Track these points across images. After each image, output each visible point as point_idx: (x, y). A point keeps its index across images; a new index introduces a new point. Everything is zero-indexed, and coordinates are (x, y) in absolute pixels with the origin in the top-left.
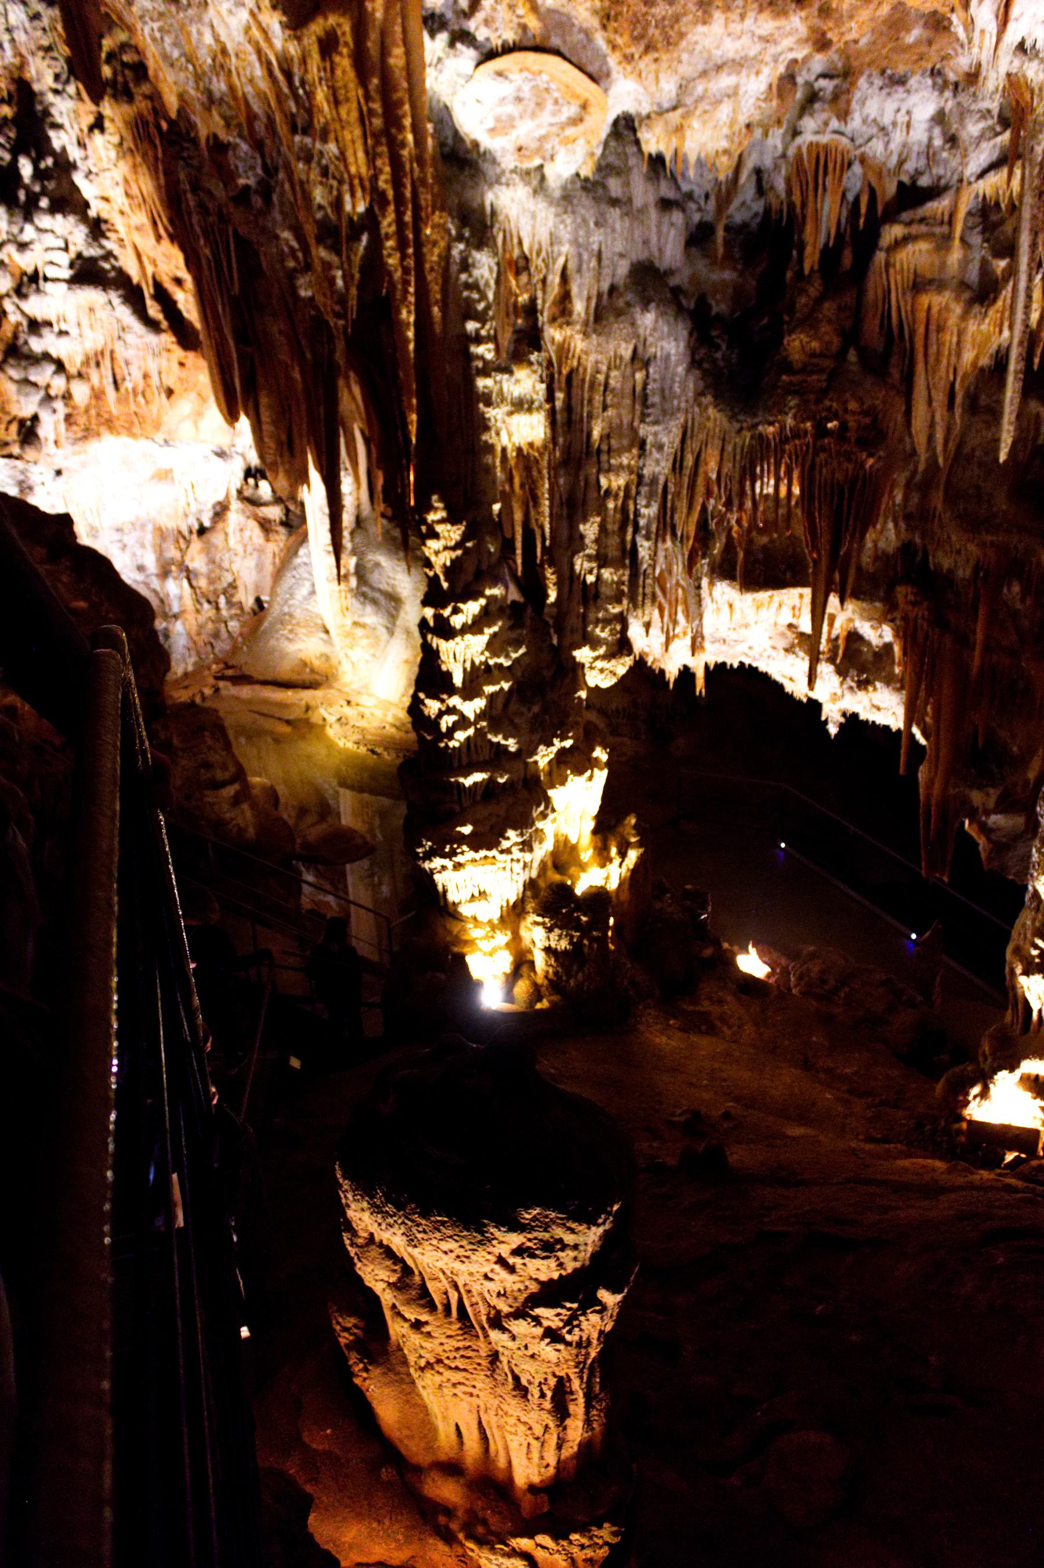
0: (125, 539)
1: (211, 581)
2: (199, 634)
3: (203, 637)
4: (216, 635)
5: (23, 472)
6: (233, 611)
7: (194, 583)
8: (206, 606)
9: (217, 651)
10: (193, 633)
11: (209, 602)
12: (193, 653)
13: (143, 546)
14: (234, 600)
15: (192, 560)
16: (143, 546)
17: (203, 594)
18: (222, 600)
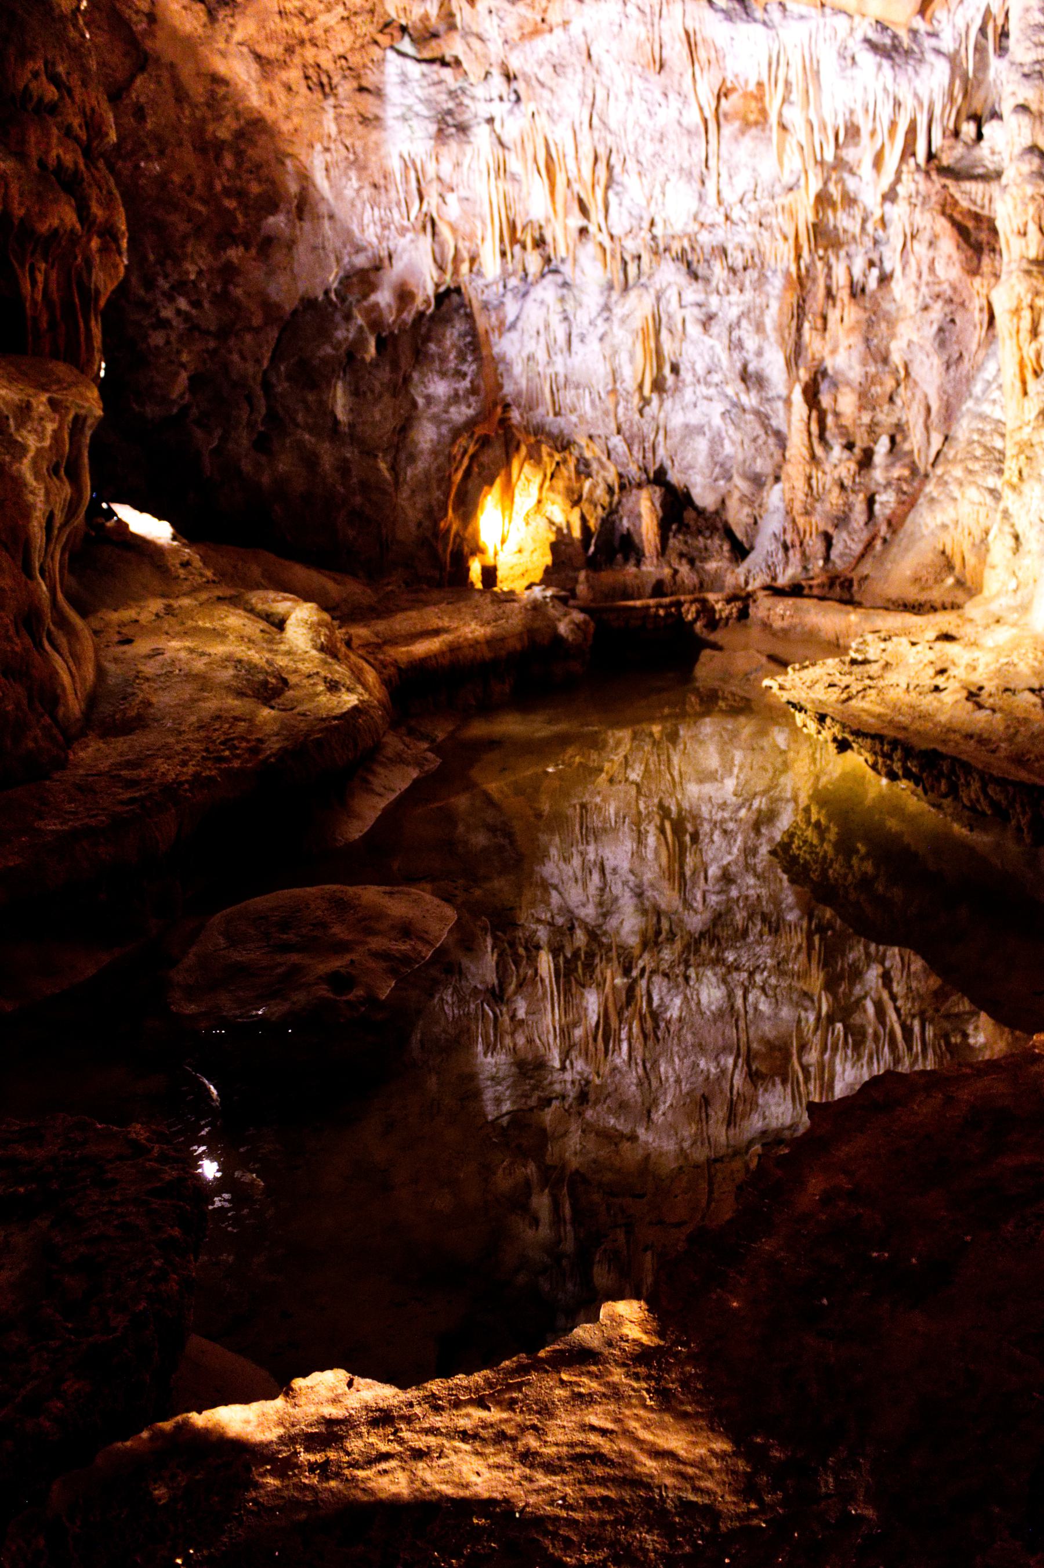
0: (714, 301)
1: (866, 401)
2: (807, 513)
3: (816, 519)
4: (842, 521)
5: (452, 94)
6: (896, 472)
7: (825, 400)
8: (837, 452)
9: (834, 554)
10: (798, 506)
11: (849, 446)
12: (795, 556)
13: (760, 328)
14: (906, 447)
15: (834, 351)
16: (760, 328)
17: (842, 428)
18: (882, 447)
